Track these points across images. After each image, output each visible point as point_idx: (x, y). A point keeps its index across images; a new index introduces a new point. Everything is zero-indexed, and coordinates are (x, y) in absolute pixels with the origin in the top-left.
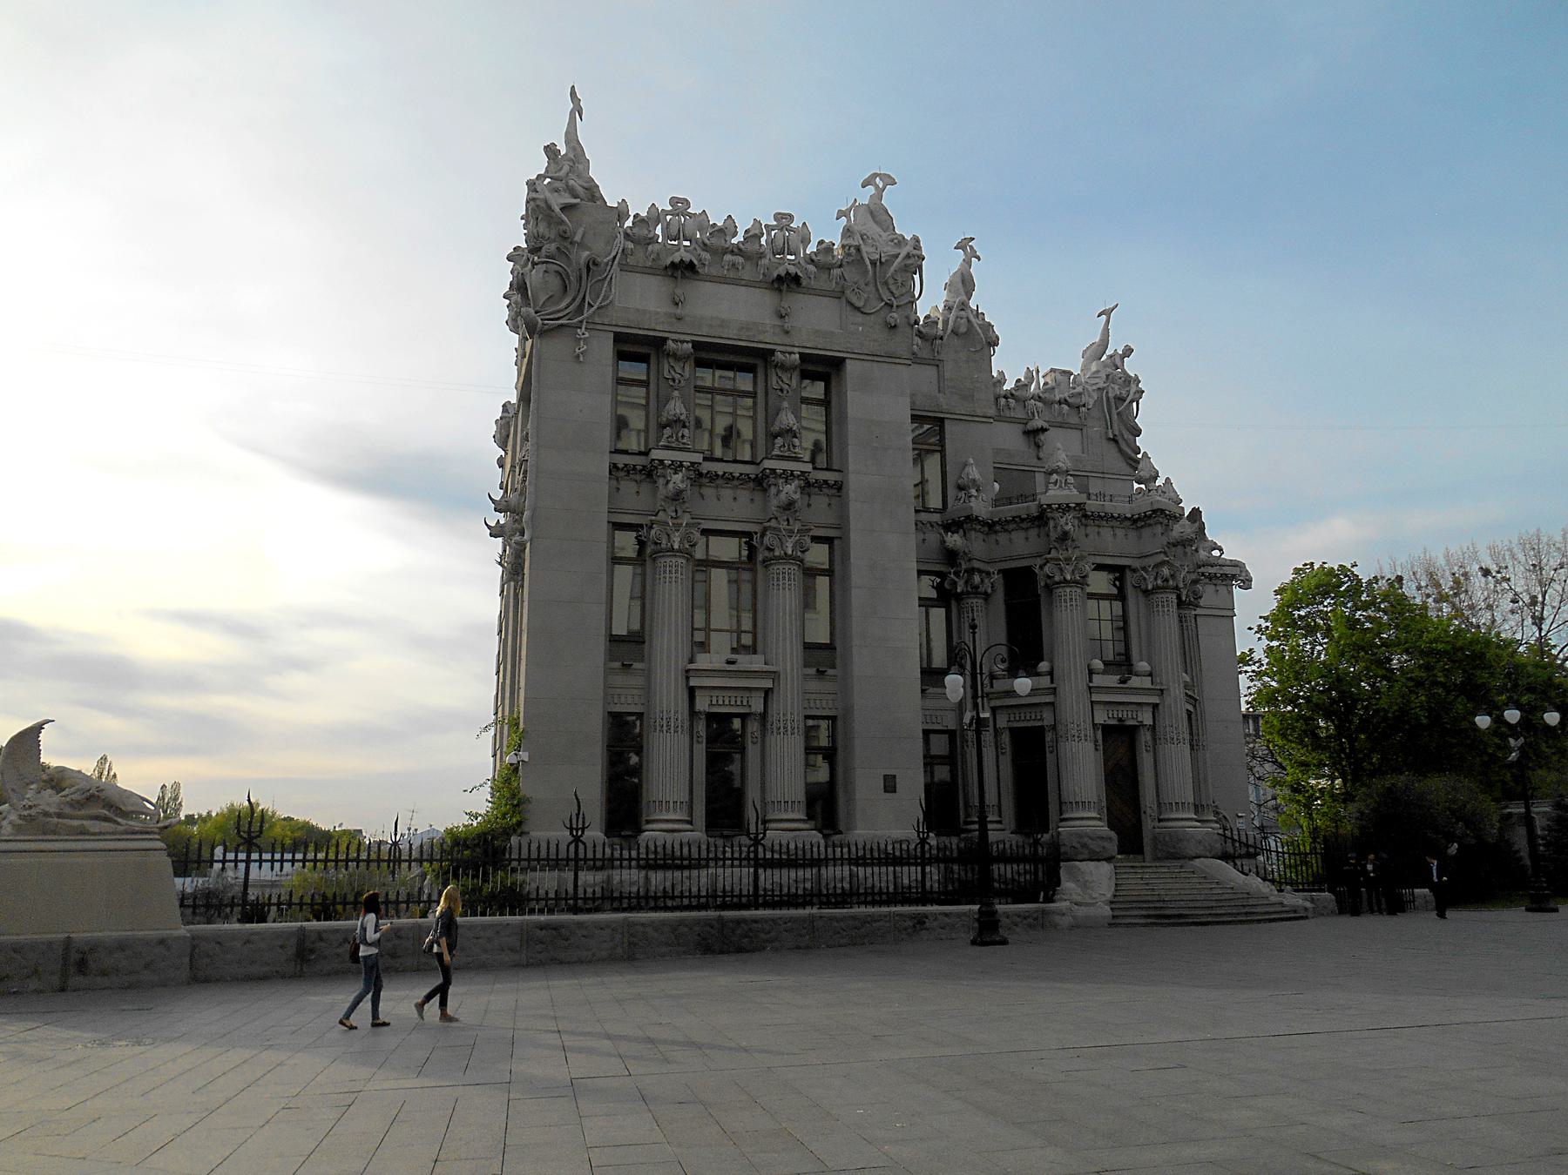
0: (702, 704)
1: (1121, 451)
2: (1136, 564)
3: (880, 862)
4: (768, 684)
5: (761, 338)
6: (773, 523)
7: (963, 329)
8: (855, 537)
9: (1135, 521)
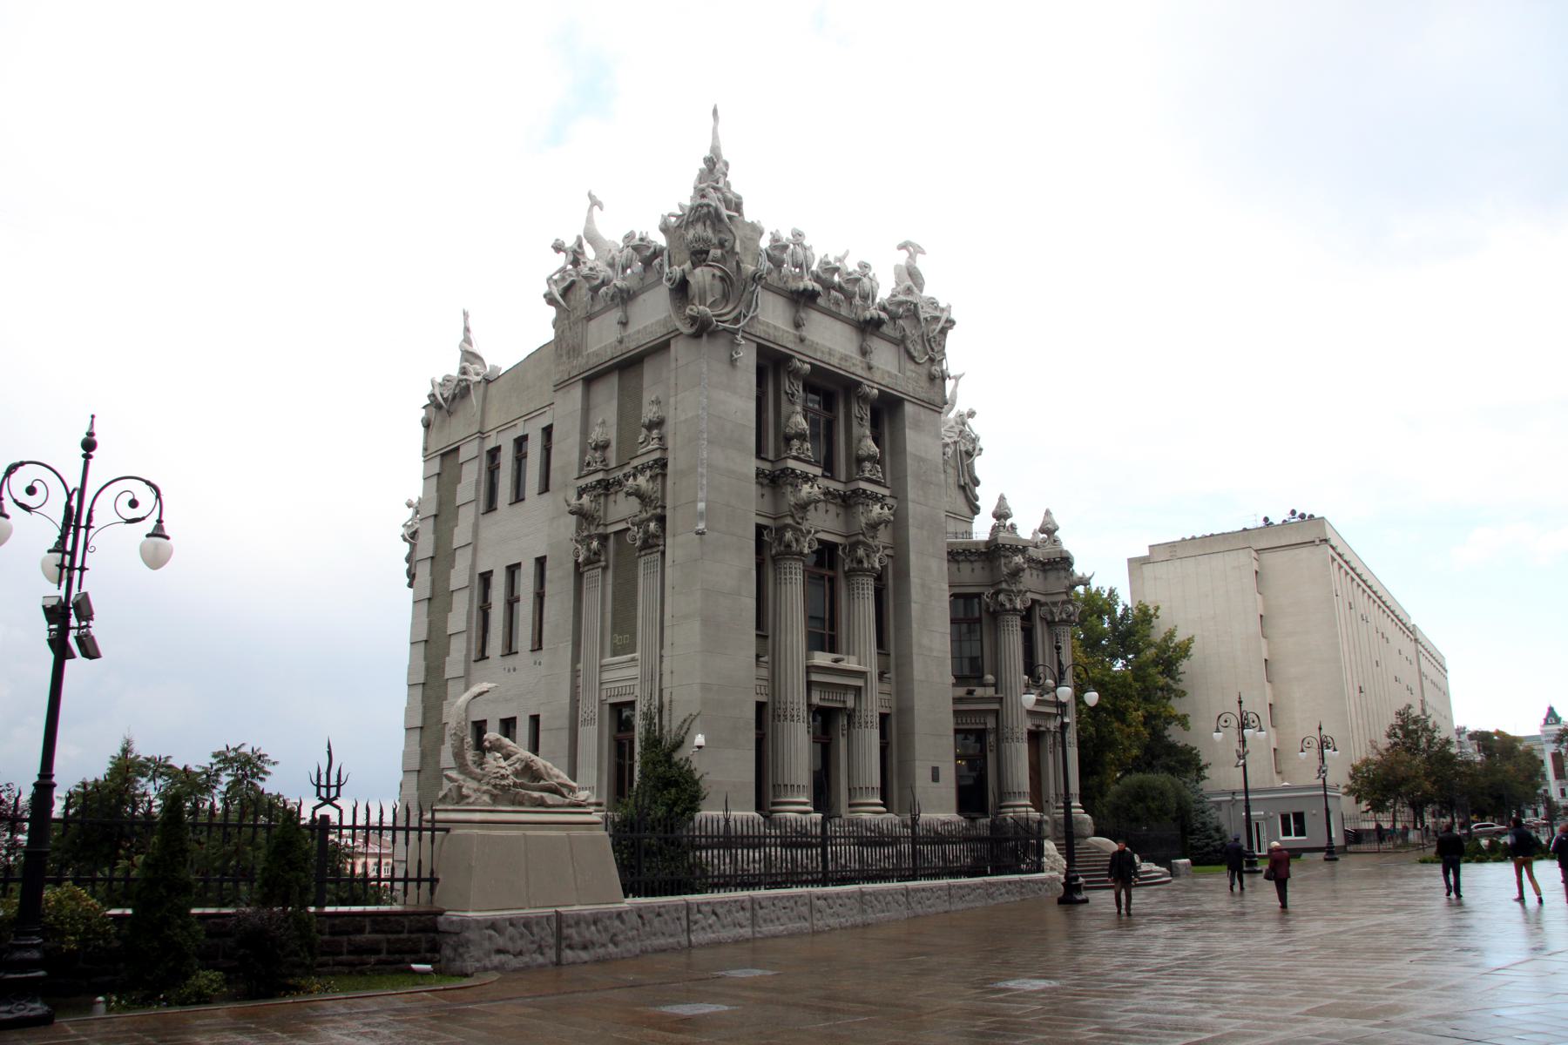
0: (816, 699)
1: (967, 497)
2: (1042, 599)
4: (860, 683)
6: (861, 538)
9: (1044, 564)
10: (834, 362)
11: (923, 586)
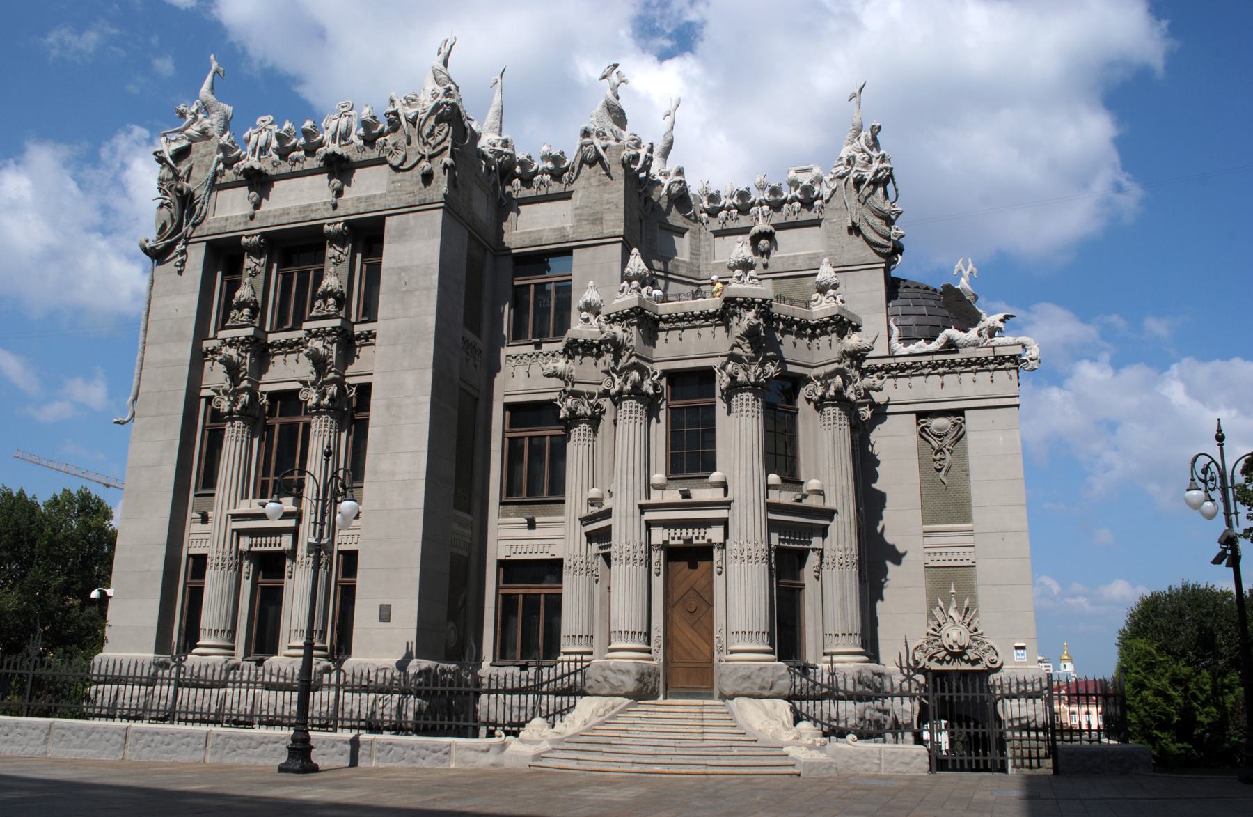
0: (245, 543)
1: (865, 238)
3: (366, 689)
5: (313, 216)
7: (591, 155)
8: (377, 381)
10: (292, 220)
11: (389, 407)
